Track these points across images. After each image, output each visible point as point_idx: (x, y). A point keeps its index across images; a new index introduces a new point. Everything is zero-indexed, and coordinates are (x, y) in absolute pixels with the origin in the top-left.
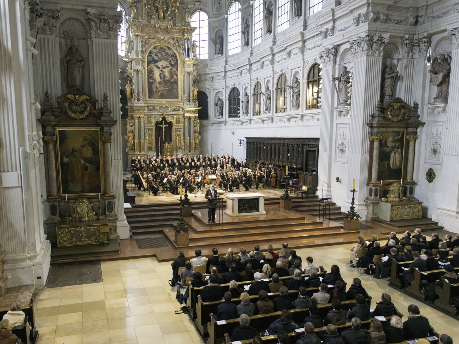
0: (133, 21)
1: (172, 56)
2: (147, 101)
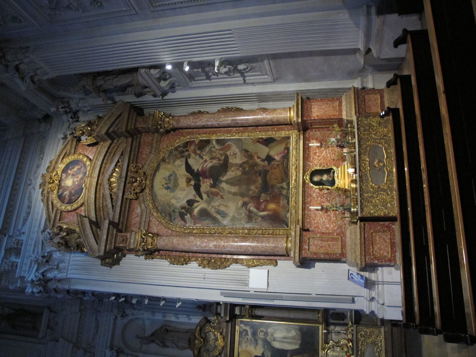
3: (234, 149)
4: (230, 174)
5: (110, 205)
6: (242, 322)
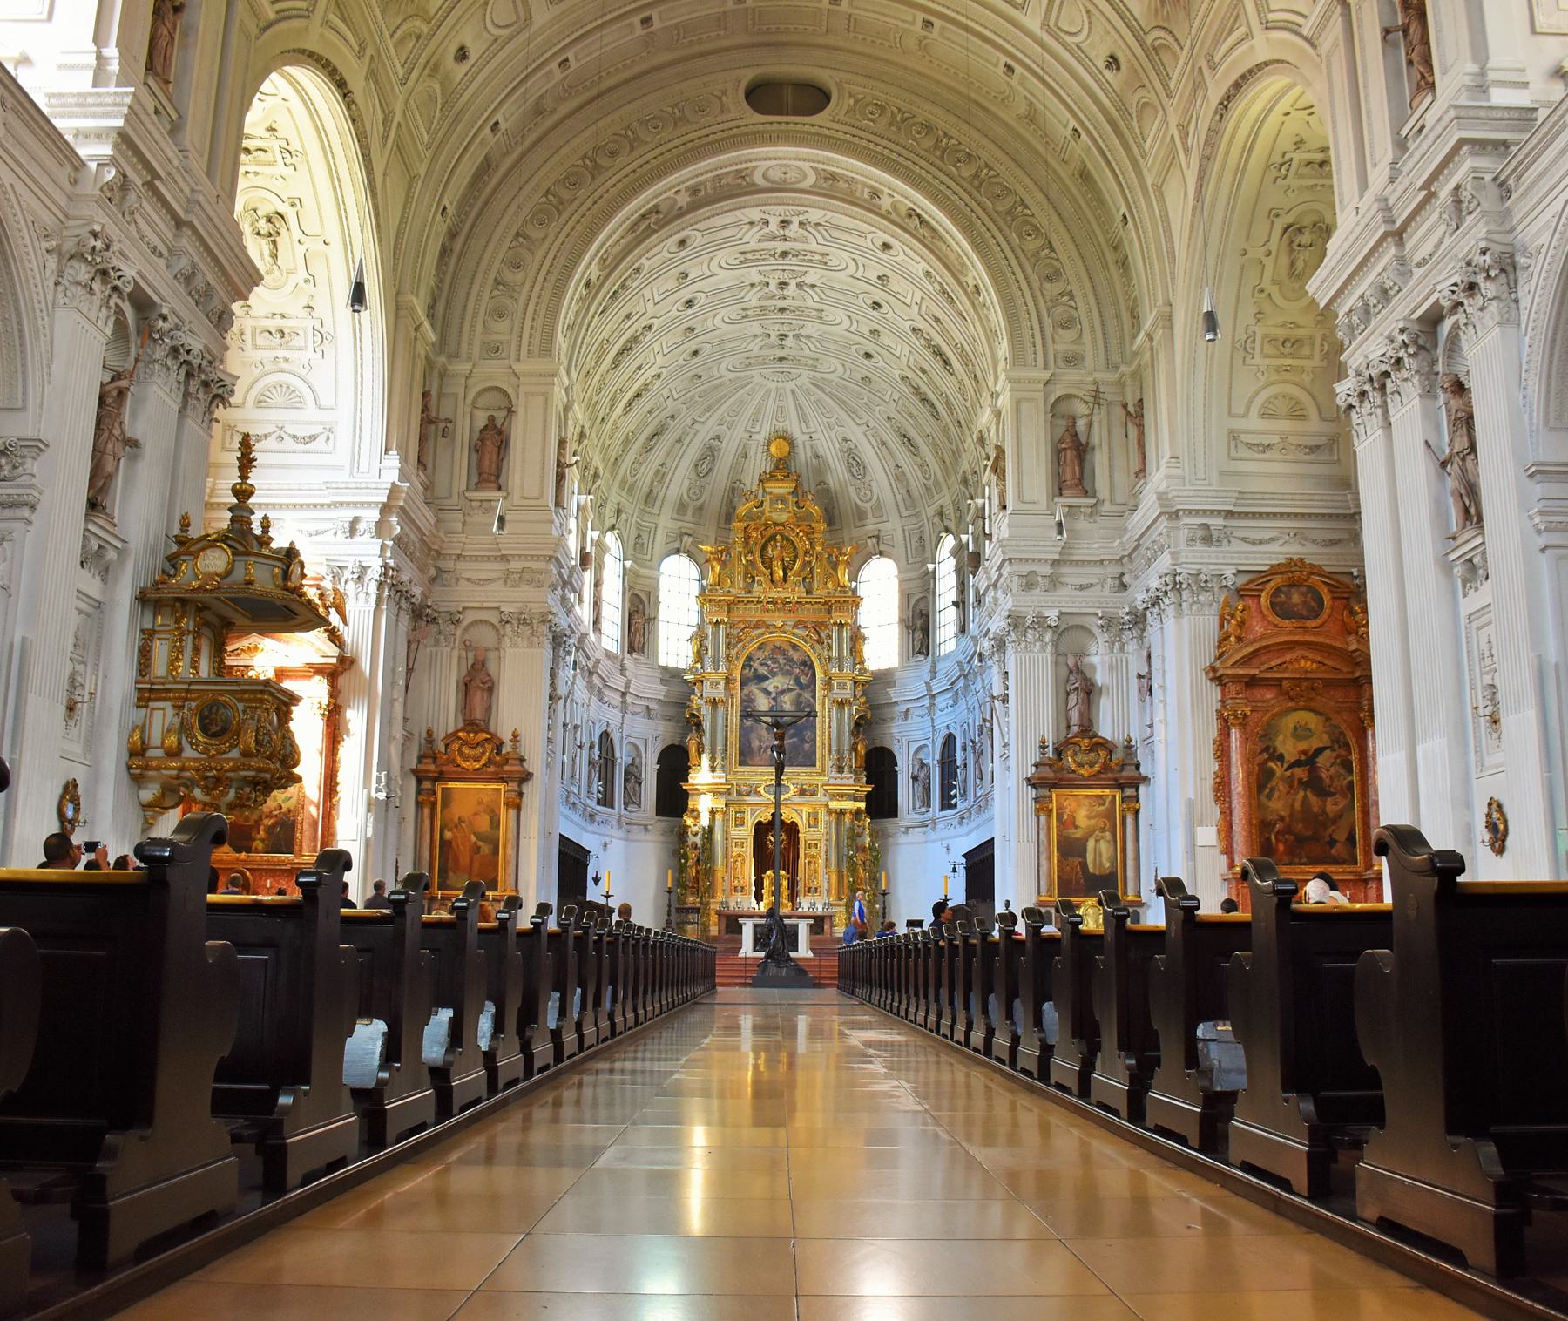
0: (710, 591)
1: (804, 663)
2: (735, 773)
3: (1343, 803)
4: (1314, 800)
5: (1273, 664)
6: (1114, 797)
